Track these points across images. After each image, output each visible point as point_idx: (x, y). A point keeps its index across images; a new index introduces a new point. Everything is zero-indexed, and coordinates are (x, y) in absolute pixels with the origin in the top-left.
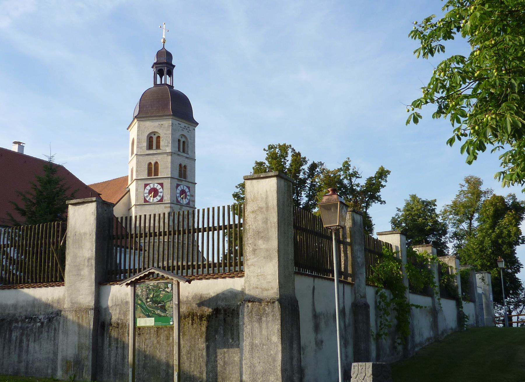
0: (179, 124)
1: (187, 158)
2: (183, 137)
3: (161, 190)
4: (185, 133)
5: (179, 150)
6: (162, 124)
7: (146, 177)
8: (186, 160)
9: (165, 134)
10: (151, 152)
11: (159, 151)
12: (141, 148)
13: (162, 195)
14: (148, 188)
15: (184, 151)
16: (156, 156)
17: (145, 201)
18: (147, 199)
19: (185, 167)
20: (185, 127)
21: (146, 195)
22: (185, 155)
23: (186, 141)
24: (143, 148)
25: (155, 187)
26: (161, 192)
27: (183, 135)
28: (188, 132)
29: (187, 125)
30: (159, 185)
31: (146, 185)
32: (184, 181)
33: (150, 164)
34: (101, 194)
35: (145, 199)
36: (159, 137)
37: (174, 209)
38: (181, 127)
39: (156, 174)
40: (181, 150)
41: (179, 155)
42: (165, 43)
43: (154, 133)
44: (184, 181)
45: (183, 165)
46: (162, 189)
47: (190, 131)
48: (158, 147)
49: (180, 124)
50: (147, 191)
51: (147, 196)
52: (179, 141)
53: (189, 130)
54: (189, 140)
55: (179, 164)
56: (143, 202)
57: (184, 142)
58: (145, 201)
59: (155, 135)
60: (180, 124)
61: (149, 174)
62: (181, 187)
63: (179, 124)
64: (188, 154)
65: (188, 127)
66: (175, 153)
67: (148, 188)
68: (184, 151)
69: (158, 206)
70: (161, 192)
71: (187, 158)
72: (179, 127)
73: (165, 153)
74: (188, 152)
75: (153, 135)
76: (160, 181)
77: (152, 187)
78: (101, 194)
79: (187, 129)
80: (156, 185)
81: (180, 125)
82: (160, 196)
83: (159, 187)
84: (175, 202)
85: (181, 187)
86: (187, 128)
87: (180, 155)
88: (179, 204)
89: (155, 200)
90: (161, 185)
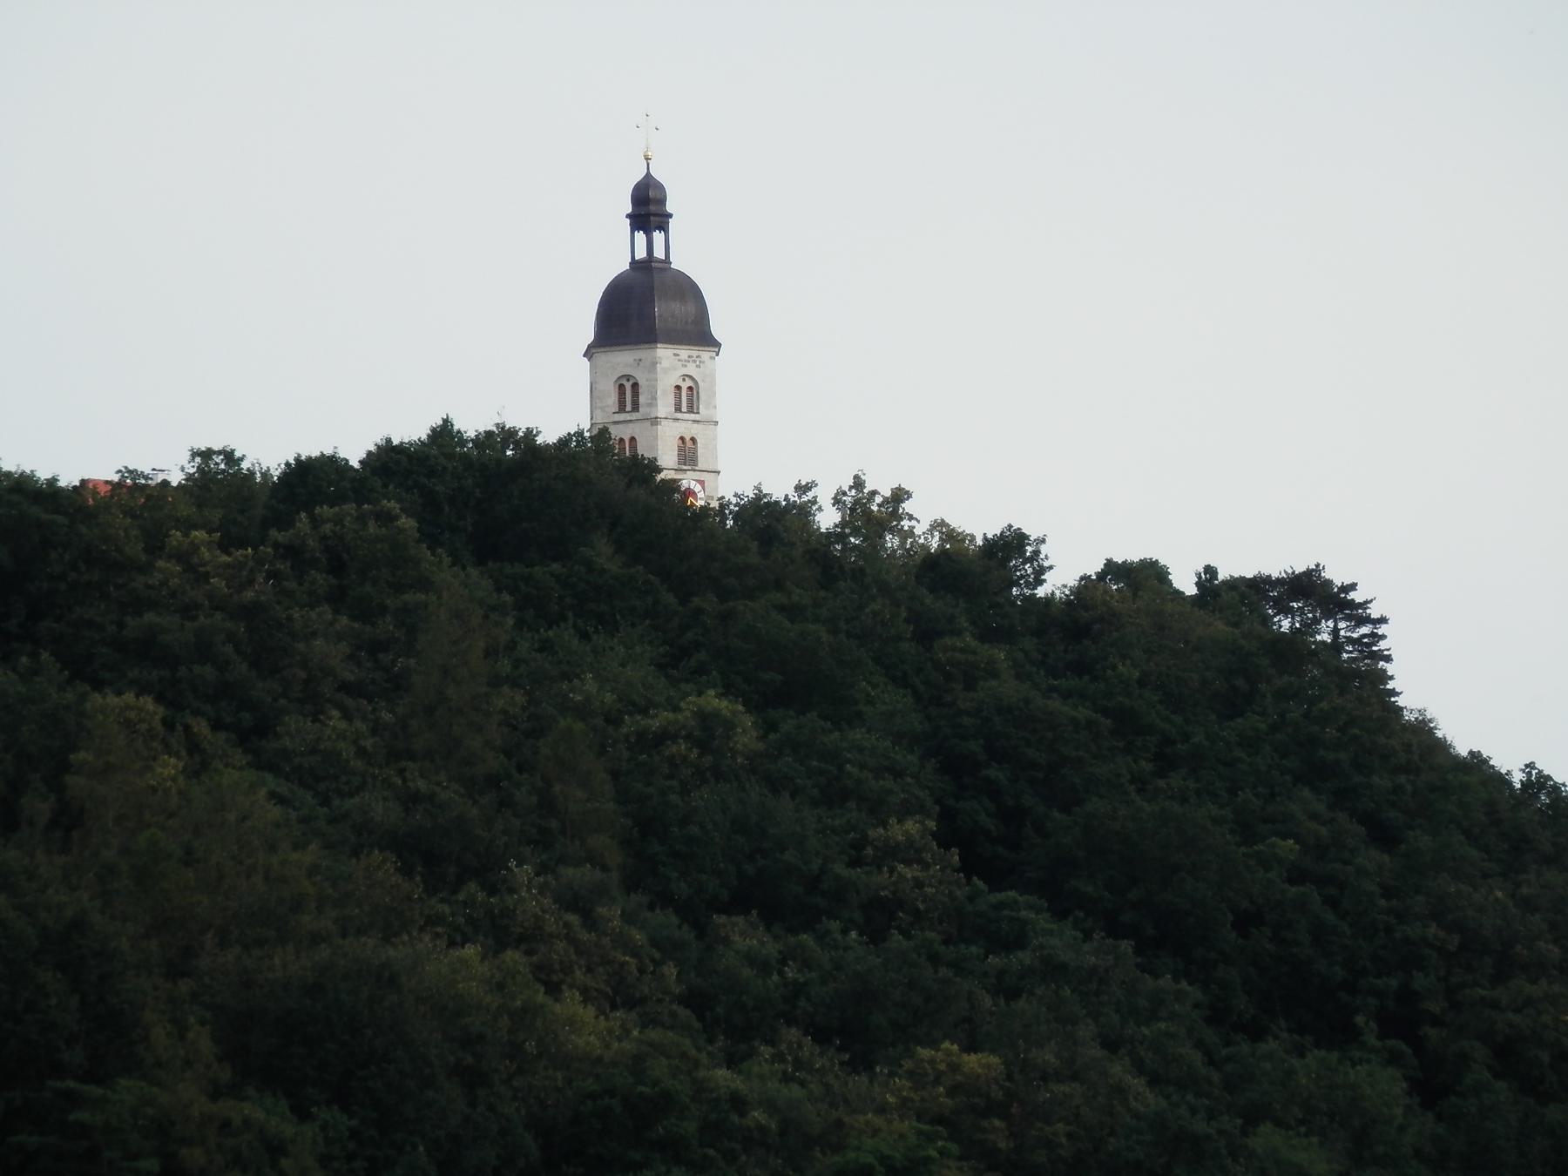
0: (675, 355)
2: (687, 379)
4: (691, 370)
5: (678, 409)
6: (640, 360)
8: (695, 425)
10: (622, 417)
11: (635, 416)
15: (691, 409)
16: (630, 425)
19: (693, 440)
20: (689, 357)
22: (692, 416)
24: (606, 409)
28: (698, 366)
29: (694, 353)
36: (635, 386)
38: (679, 360)
40: (684, 409)
43: (628, 377)
45: (688, 439)
47: (704, 362)
48: (636, 407)
49: (678, 355)
52: (678, 388)
59: (628, 380)
60: (678, 355)
63: (675, 355)
64: (698, 413)
65: (697, 357)
68: (691, 409)
72: (677, 361)
74: (698, 408)
75: (624, 382)
79: (695, 361)
81: (678, 358)
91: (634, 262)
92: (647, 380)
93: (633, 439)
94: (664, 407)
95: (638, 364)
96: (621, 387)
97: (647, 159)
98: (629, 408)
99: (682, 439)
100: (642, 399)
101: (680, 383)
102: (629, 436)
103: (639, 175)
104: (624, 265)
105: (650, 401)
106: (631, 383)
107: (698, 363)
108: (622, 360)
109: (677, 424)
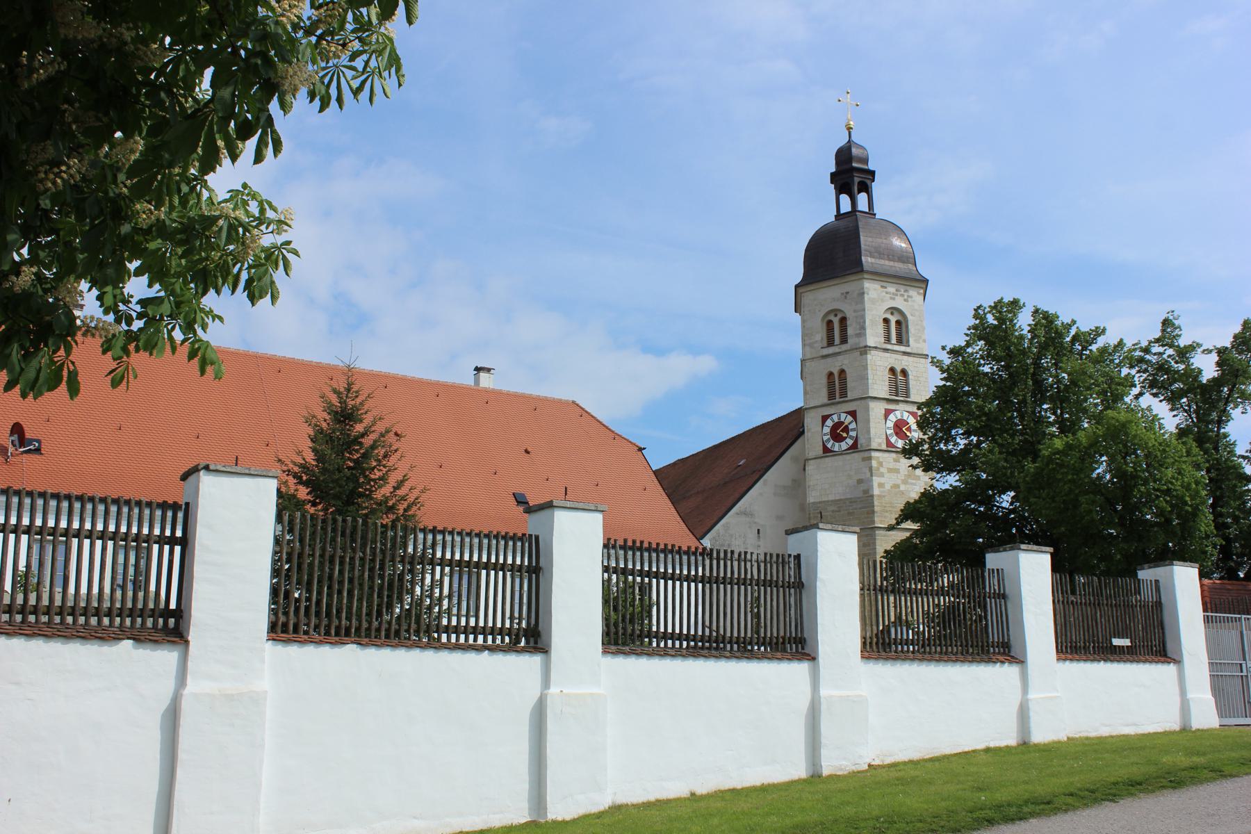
1: (905, 353)
4: (899, 303)
5: (888, 340)
6: (847, 293)
7: (825, 400)
8: (906, 358)
9: (855, 311)
10: (831, 350)
11: (844, 347)
12: (811, 345)
13: (855, 435)
14: (829, 423)
17: (826, 450)
18: (829, 446)
19: (904, 372)
21: (825, 438)
22: (902, 348)
23: (903, 321)
24: (815, 345)
27: (893, 310)
28: (905, 300)
29: (902, 289)
30: (849, 416)
31: (825, 418)
32: (902, 401)
33: (831, 374)
34: (644, 449)
35: (825, 447)
36: (843, 320)
37: (881, 460)
38: (887, 293)
39: (844, 393)
40: (894, 340)
41: (886, 350)
43: (835, 312)
44: (902, 401)
45: (898, 369)
46: (854, 423)
48: (844, 340)
50: (827, 430)
51: (828, 440)
52: (886, 321)
53: (908, 296)
54: (910, 317)
55: (889, 367)
56: (819, 450)
57: (898, 323)
58: (826, 450)
59: (836, 315)
61: (831, 395)
62: (895, 415)
64: (909, 346)
66: (876, 348)
67: (829, 423)
68: (900, 341)
69: (848, 457)
71: (905, 353)
73: (857, 349)
74: (908, 341)
75: (832, 317)
76: (850, 407)
77: (836, 420)
78: (644, 449)
79: (902, 295)
80: (843, 416)
82: (851, 437)
83: (850, 418)
84: (884, 447)
85: (895, 415)
86: (902, 293)
87: (888, 350)
88: (893, 450)
89: (844, 446)
91: (839, 216)
92: (855, 311)
93: (842, 372)
94: (874, 336)
95: (846, 297)
96: (830, 323)
97: (849, 129)
98: (837, 340)
99: (892, 370)
100: (850, 331)
101: (888, 316)
102: (838, 368)
103: (843, 141)
104: (830, 217)
105: (858, 332)
106: (839, 316)
107: (906, 297)
108: (828, 295)
109: (887, 355)
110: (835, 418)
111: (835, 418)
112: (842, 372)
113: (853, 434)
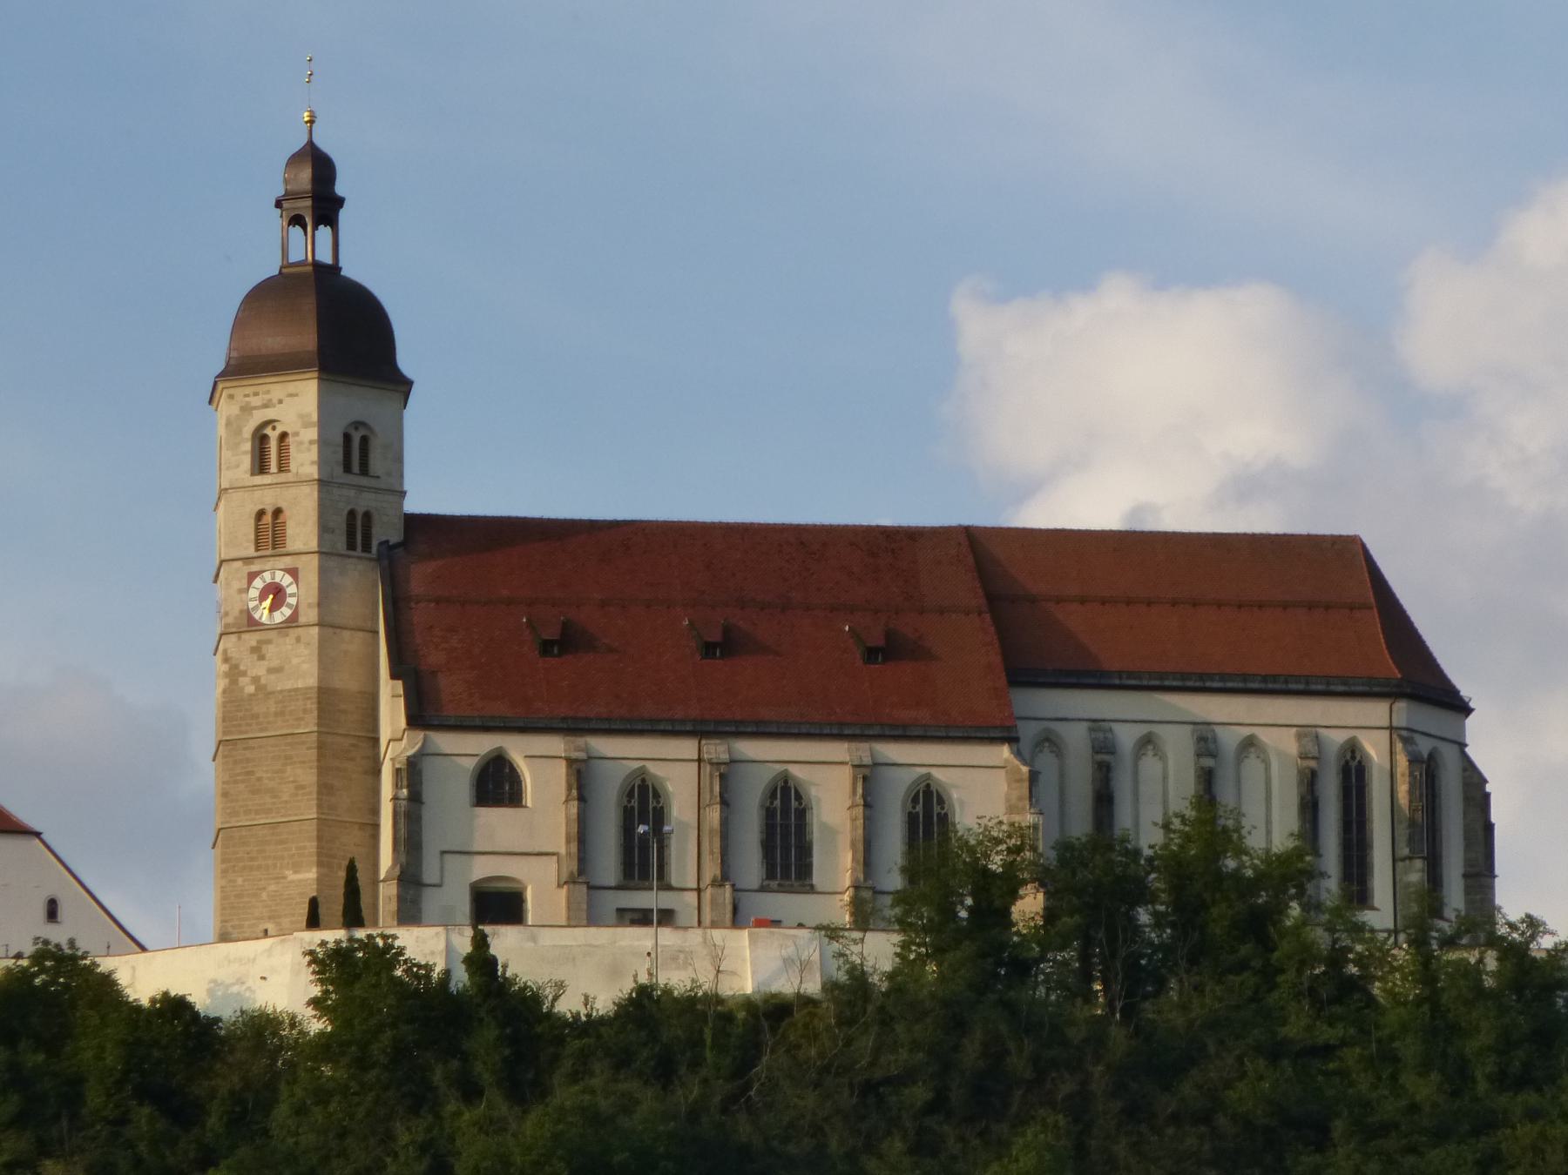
3: (292, 590)
7: (251, 552)
11: (283, 477)
13: (295, 604)
14: (258, 583)
25: (277, 580)
26: (292, 595)
30: (287, 576)
31: (252, 576)
33: (260, 514)
42: (314, 125)
46: (294, 585)
48: (283, 467)
50: (254, 594)
67: (258, 583)
70: (292, 595)
75: (268, 431)
77: (268, 580)
80: (279, 574)
82: (289, 606)
90: (293, 572)
93: (278, 512)
98: (274, 468)
110: (267, 576)
111: (267, 576)
112: (278, 512)
113: (292, 601)
